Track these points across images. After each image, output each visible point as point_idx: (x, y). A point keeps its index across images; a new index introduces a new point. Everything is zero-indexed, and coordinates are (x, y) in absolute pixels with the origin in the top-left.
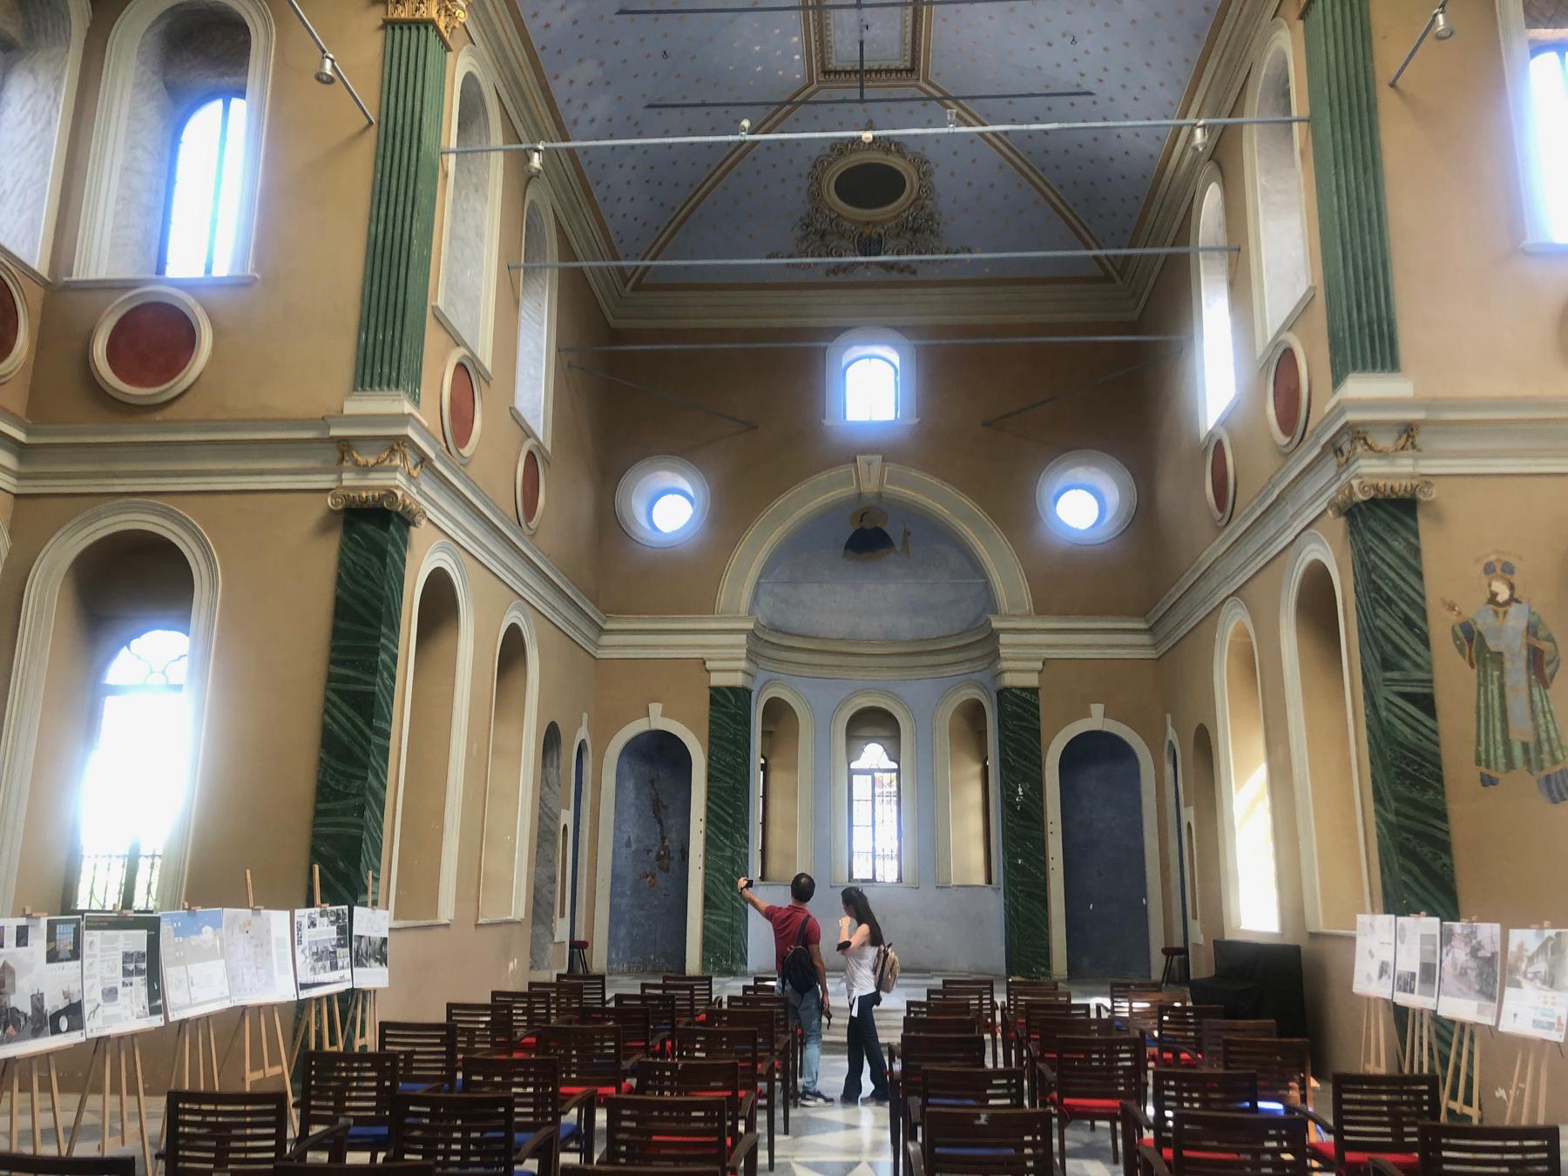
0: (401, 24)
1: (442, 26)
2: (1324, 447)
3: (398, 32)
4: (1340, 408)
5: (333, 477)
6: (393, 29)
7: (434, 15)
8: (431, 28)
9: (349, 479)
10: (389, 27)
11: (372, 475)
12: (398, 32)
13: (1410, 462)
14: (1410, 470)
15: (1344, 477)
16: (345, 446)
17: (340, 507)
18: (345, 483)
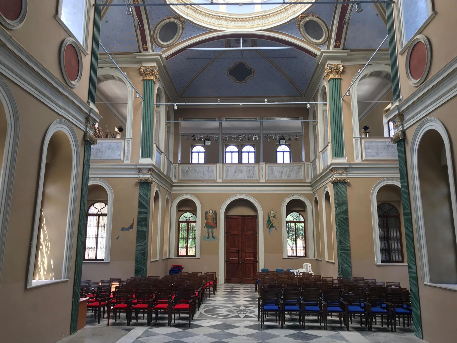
0: (146, 80)
1: (154, 80)
2: (330, 170)
3: (146, 82)
4: (332, 164)
5: (137, 175)
6: (145, 81)
7: (153, 79)
8: (152, 81)
9: (141, 176)
10: (144, 81)
11: (145, 175)
12: (146, 82)
13: (346, 175)
14: (345, 176)
15: (333, 176)
16: (140, 170)
17: (139, 181)
18: (140, 177)
